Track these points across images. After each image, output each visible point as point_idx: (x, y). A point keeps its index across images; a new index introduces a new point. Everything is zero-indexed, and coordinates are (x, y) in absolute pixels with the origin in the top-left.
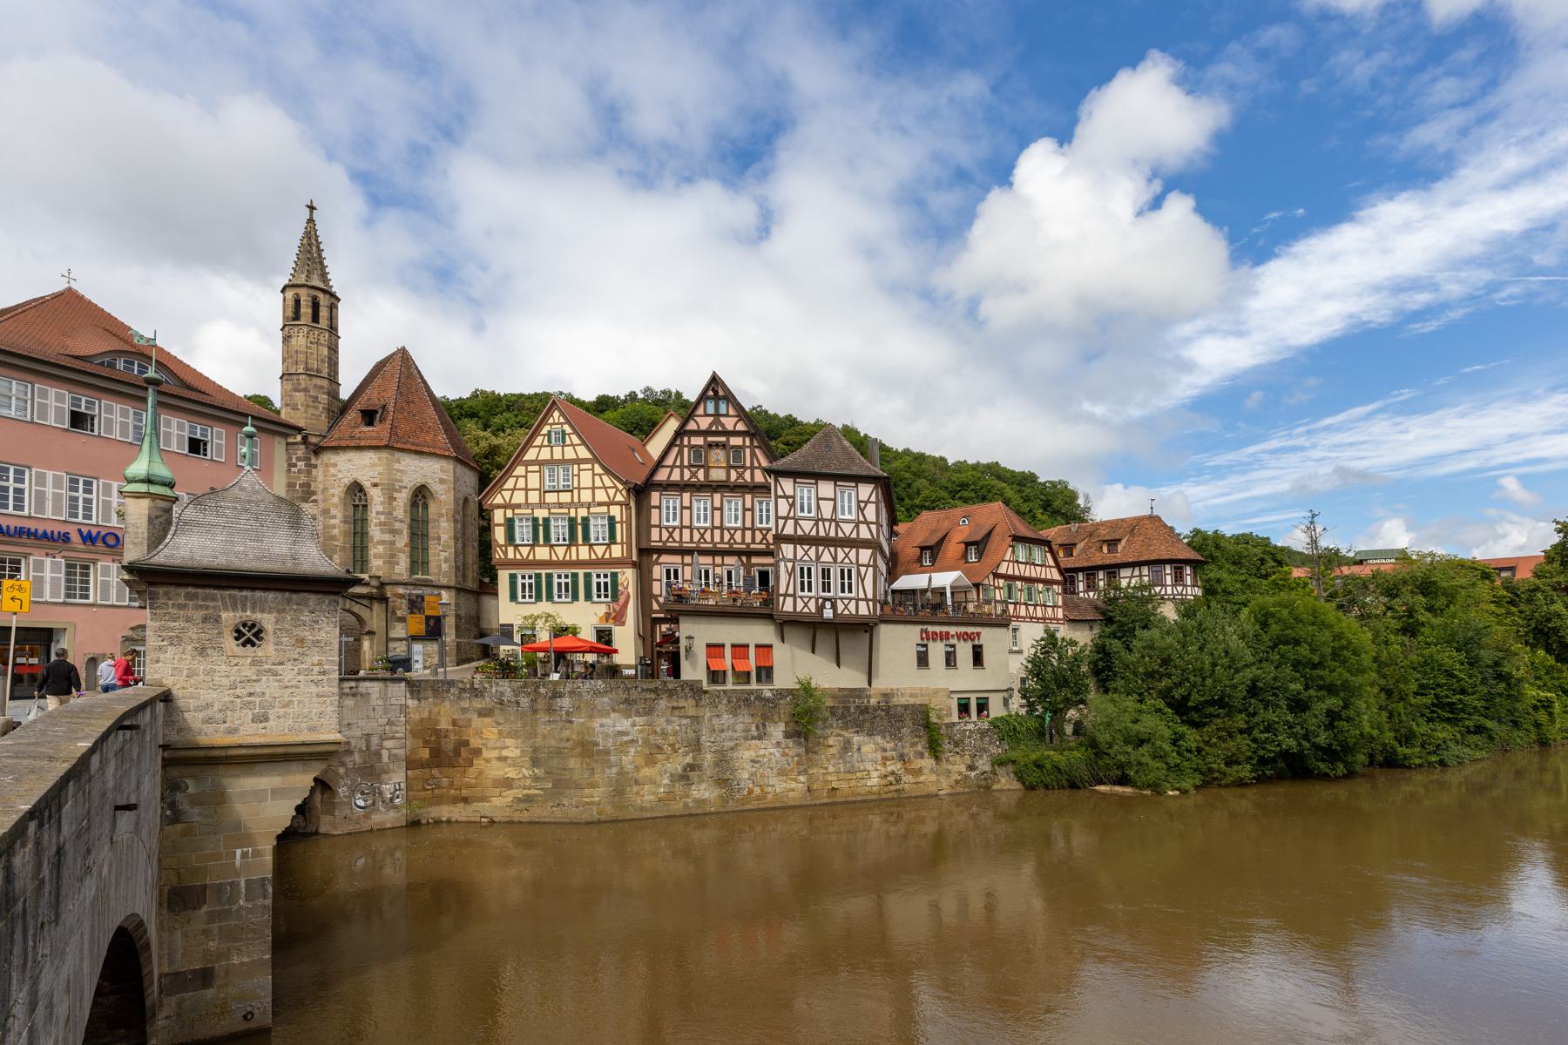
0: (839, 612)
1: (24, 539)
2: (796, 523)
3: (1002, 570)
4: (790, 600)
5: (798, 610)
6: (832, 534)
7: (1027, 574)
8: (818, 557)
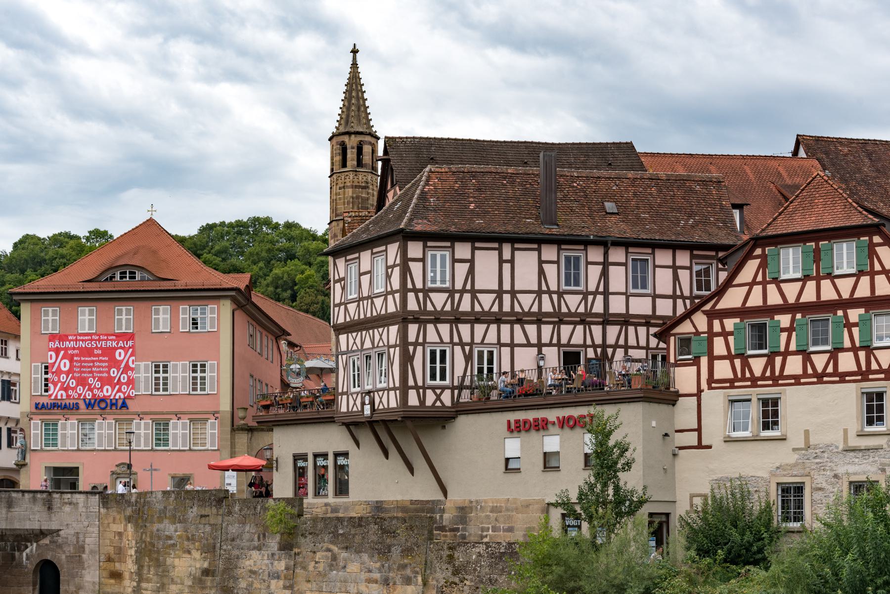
0: (376, 408)
1: (56, 411)
2: (346, 309)
3: (732, 299)
4: (345, 397)
5: (350, 410)
6: (369, 315)
7: (809, 296)
8: (362, 344)
